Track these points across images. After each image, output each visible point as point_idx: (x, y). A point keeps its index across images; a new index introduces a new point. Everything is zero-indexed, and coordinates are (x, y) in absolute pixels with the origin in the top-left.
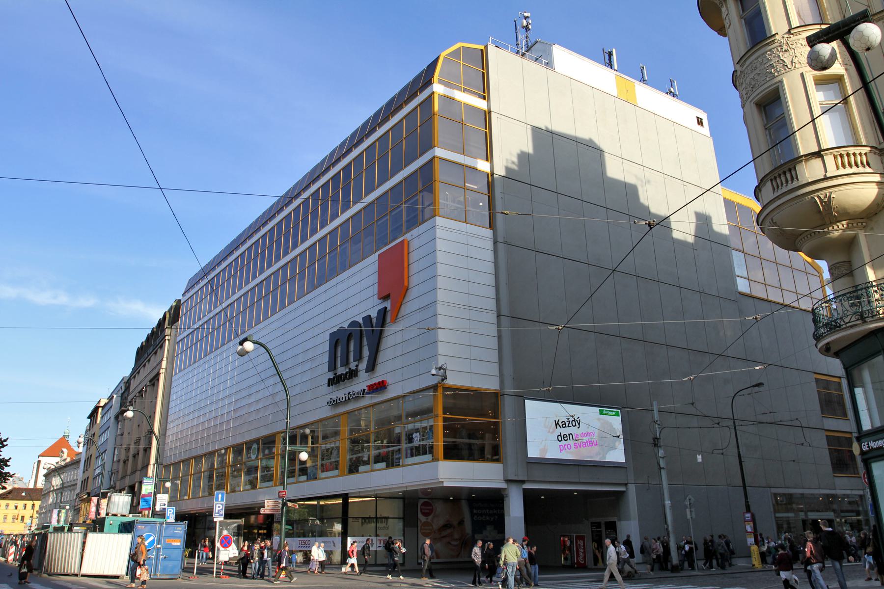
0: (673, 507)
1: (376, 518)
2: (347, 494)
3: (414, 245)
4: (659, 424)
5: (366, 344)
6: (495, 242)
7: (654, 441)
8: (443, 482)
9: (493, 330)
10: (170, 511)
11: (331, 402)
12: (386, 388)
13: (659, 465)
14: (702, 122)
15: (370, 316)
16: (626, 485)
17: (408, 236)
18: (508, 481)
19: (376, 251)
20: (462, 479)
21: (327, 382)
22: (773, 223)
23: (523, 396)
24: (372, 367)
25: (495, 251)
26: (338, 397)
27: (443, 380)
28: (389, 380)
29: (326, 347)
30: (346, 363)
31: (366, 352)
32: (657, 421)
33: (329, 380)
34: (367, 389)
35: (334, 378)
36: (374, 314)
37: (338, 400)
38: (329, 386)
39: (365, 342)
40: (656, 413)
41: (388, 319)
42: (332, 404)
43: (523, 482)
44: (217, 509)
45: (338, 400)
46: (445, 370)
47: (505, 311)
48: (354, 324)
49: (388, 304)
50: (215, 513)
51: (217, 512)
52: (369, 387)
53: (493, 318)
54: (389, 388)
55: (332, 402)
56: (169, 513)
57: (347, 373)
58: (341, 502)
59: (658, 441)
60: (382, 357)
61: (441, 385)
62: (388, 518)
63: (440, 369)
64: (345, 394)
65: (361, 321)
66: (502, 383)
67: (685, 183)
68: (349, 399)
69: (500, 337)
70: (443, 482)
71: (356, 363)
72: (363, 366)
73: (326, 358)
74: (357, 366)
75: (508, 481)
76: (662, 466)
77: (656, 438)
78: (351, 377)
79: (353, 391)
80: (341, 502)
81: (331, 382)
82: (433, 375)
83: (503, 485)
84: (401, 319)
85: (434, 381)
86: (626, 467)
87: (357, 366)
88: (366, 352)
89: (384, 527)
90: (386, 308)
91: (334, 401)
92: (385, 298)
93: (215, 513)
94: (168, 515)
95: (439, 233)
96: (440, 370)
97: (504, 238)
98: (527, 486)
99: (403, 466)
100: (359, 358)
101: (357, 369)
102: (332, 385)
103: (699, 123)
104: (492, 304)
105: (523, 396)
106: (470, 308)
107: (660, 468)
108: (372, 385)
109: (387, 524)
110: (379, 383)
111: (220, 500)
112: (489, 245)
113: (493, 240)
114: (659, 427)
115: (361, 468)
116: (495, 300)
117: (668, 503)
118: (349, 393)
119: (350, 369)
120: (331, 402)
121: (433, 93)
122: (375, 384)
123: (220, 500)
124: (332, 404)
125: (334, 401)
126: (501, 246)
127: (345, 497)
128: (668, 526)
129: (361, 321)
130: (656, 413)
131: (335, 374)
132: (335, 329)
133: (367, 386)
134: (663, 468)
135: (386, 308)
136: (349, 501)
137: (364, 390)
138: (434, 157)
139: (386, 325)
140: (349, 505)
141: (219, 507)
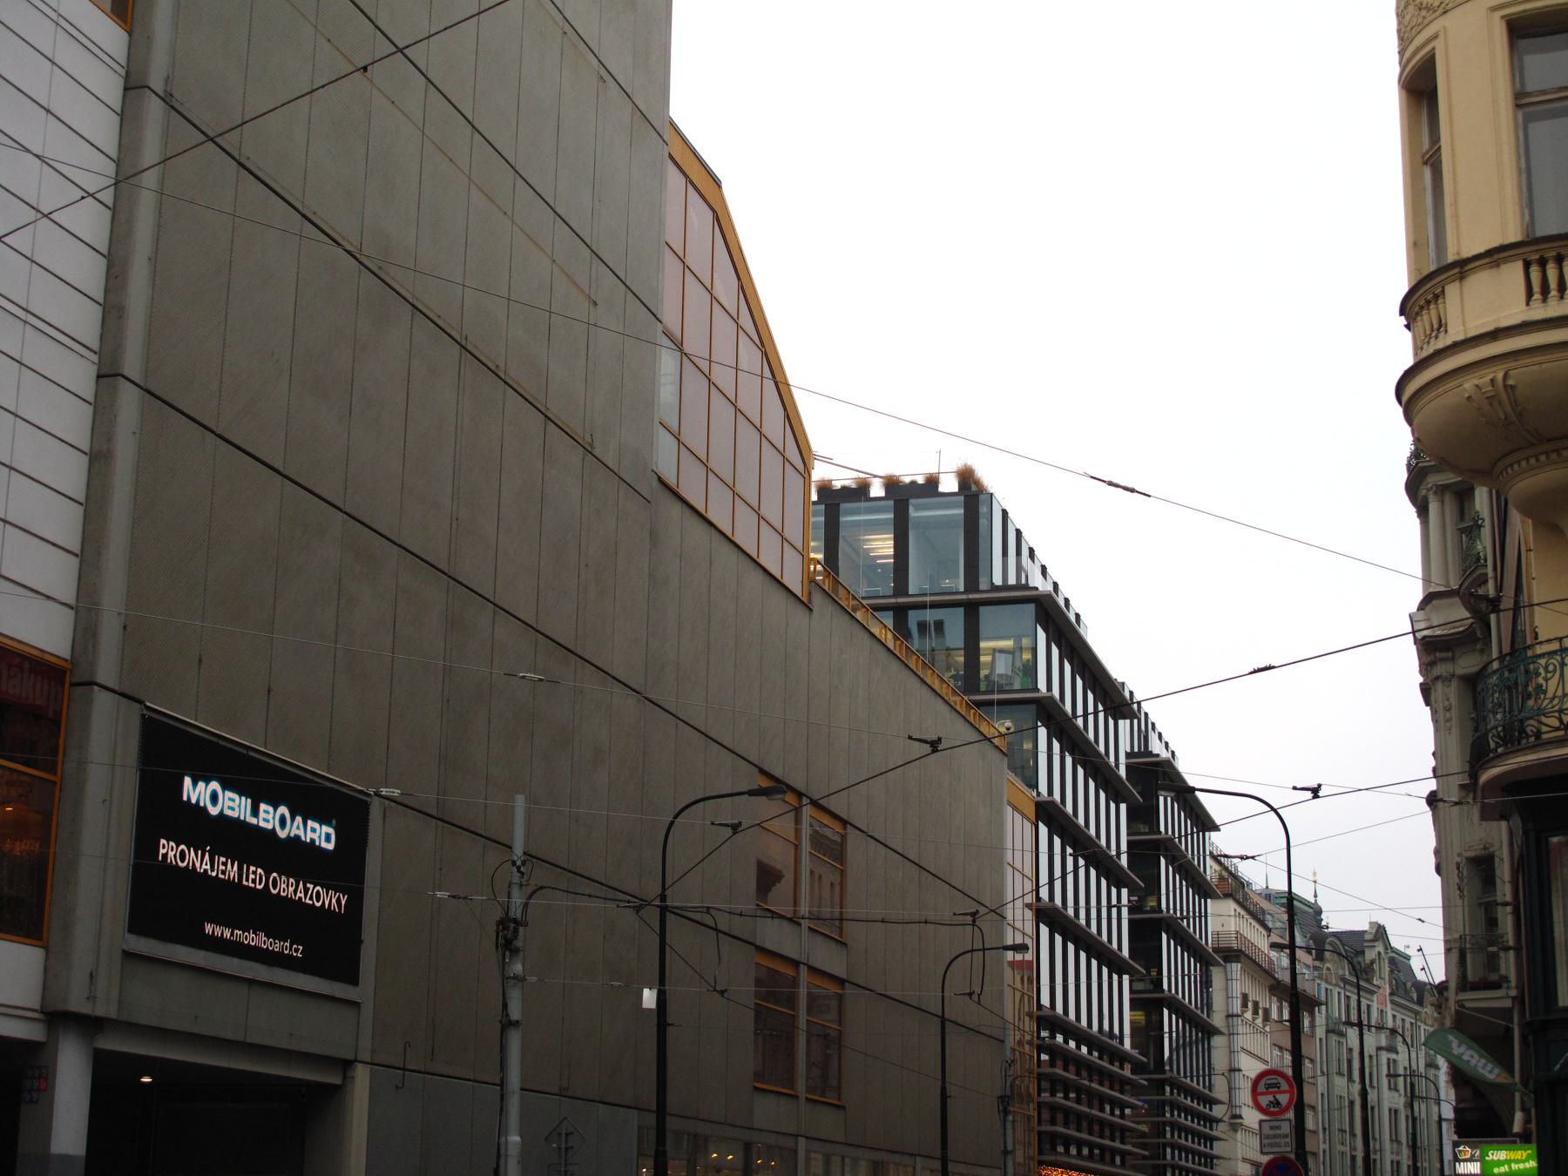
6: (133, 85)
16: (346, 1065)
18: (56, 1018)
22: (1505, 386)
25: (128, 117)
47: (132, 365)
53: (80, 374)
86: (356, 1005)
98: (111, 1043)
105: (140, 702)
107: (507, 1024)
112: (110, 87)
113: (123, 72)
134: (517, 1023)
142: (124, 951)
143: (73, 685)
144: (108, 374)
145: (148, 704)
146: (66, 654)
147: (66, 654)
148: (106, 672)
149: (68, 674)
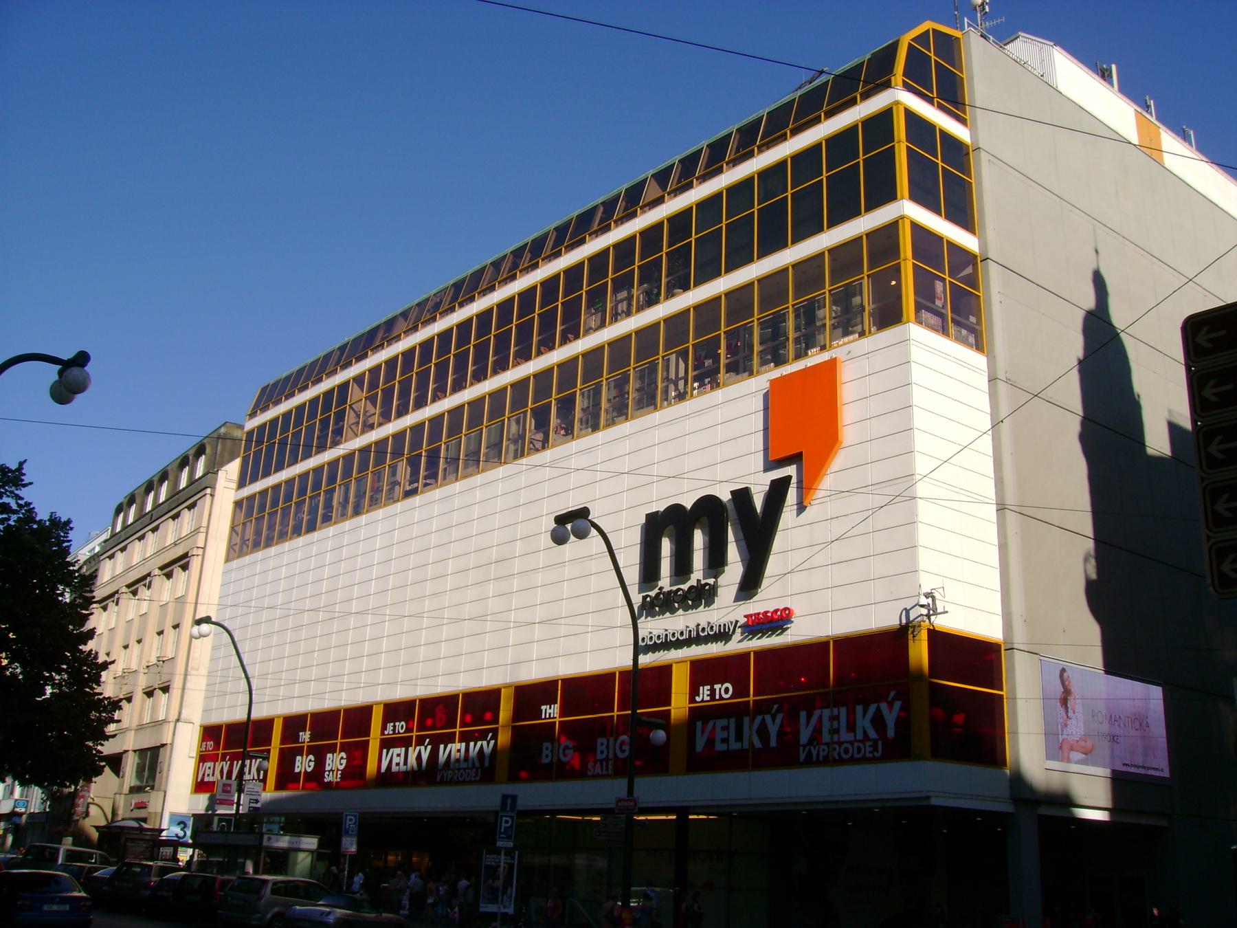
6: (992, 379)
8: (928, 798)
10: (351, 820)
11: (651, 638)
20: (955, 794)
24: (750, 585)
44: (504, 825)
47: (1010, 499)
50: (500, 833)
51: (502, 830)
56: (348, 823)
60: (773, 566)
63: (927, 595)
70: (928, 798)
83: (1008, 808)
93: (500, 833)
94: (347, 827)
95: (916, 353)
97: (1006, 372)
100: (716, 561)
111: (508, 809)
120: (651, 638)
123: (508, 809)
126: (1002, 388)
127: (683, 811)
129: (725, 497)
132: (661, 507)
141: (507, 822)
144: (1001, 508)
148: (1019, 639)
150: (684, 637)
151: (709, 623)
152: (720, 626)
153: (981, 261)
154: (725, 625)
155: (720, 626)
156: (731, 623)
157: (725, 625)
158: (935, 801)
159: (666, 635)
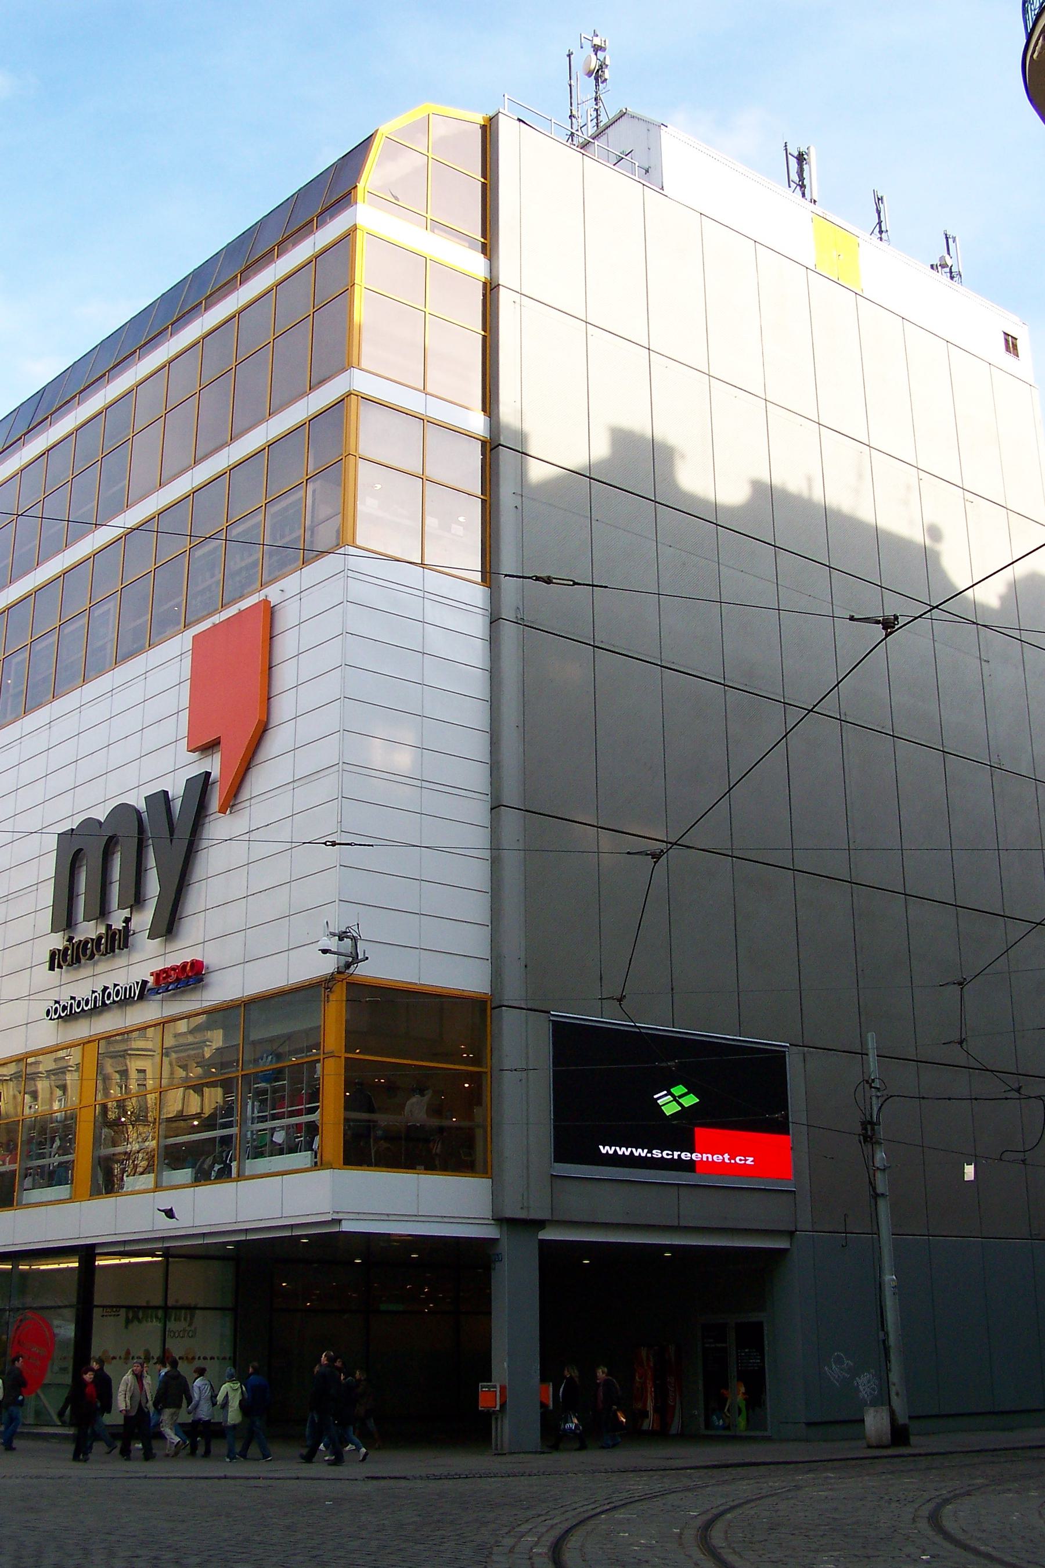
0: (899, 1289)
1: (166, 1308)
2: (92, 1247)
3: (287, 618)
4: (878, 1089)
5: (155, 865)
6: (494, 620)
7: (865, 1129)
9: (478, 838)
12: (202, 980)
13: (874, 1189)
14: (1015, 346)
15: (166, 793)
17: (273, 593)
19: (187, 626)
21: (48, 959)
23: (549, 1012)
25: (493, 641)
26: (73, 998)
27: (348, 966)
28: (209, 956)
29: (49, 867)
30: (103, 913)
31: (153, 887)
32: (873, 1081)
33: (53, 954)
34: (151, 980)
35: (66, 949)
36: (176, 788)
37: (75, 1006)
38: (52, 968)
39: (151, 861)
40: (872, 1060)
41: (215, 802)
42: (60, 1017)
43: (540, 1224)
45: (75, 1006)
46: (354, 939)
47: (511, 795)
48: (123, 809)
49: (213, 765)
52: (157, 975)
53: (478, 811)
54: (213, 978)
55: (60, 1009)
57: (100, 938)
58: (77, 1265)
59: (873, 1129)
61: (342, 976)
62: (196, 1308)
64: (93, 992)
65: (141, 806)
66: (496, 975)
67: (968, 495)
68: (103, 1002)
69: (496, 862)
71: (126, 913)
72: (143, 920)
73: (47, 895)
74: (127, 920)
75: (500, 1221)
76: (880, 1189)
77: (871, 1123)
78: (111, 950)
79: (115, 985)
80: (77, 1265)
81: (57, 960)
82: (325, 951)
83: (490, 1232)
84: (247, 804)
85: (328, 965)
87: (127, 920)
88: (153, 887)
89: (184, 1330)
90: (208, 774)
91: (64, 1008)
92: (207, 748)
96: (341, 939)
98: (548, 1234)
99: (241, 1177)
100: (137, 901)
101: (126, 928)
102: (60, 967)
103: (1007, 349)
104: (477, 777)
105: (549, 1012)
106: (425, 784)
107: (876, 1196)
108: (164, 971)
109: (190, 1325)
110: (185, 965)
112: (477, 625)
113: (488, 614)
114: (879, 1094)
115: (131, 1182)
116: (488, 766)
117: (890, 1278)
118: (106, 988)
119: (109, 927)
121: (354, 228)
122: (173, 969)
124: (60, 1017)
125: (64, 1008)
126: (509, 632)
127: (87, 1253)
128: (887, 1334)
129: (141, 806)
130: (872, 1060)
131: (70, 939)
133: (152, 974)
135: (208, 774)
136: (97, 1263)
137: (145, 983)
138: (349, 394)
139: (207, 820)
140: (97, 1272)
142: (552, 1175)
143: (493, 1009)
144: (495, 807)
145: (552, 1013)
146: (488, 990)
147: (488, 990)
149: (489, 1002)
150: (89, 1007)
151: (115, 985)
152: (126, 988)
153: (491, 450)
154: (131, 987)
155: (126, 988)
156: (138, 983)
157: (131, 987)
158: (347, 1227)
159: (71, 1004)
